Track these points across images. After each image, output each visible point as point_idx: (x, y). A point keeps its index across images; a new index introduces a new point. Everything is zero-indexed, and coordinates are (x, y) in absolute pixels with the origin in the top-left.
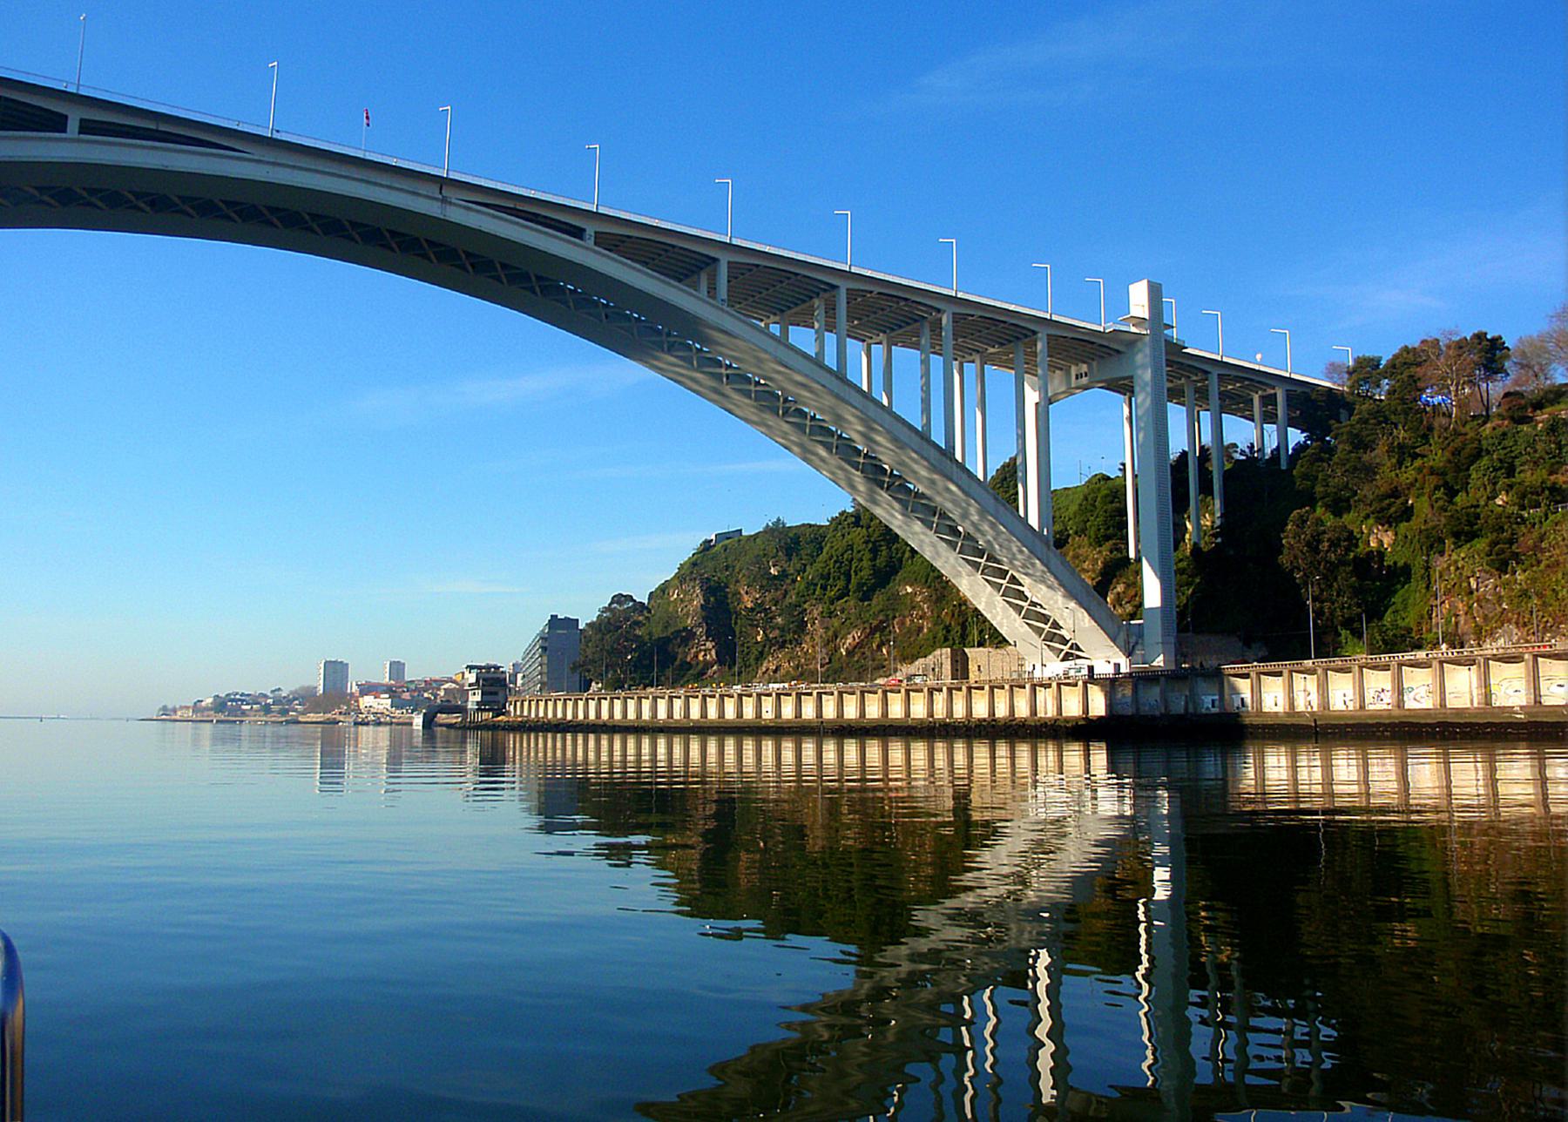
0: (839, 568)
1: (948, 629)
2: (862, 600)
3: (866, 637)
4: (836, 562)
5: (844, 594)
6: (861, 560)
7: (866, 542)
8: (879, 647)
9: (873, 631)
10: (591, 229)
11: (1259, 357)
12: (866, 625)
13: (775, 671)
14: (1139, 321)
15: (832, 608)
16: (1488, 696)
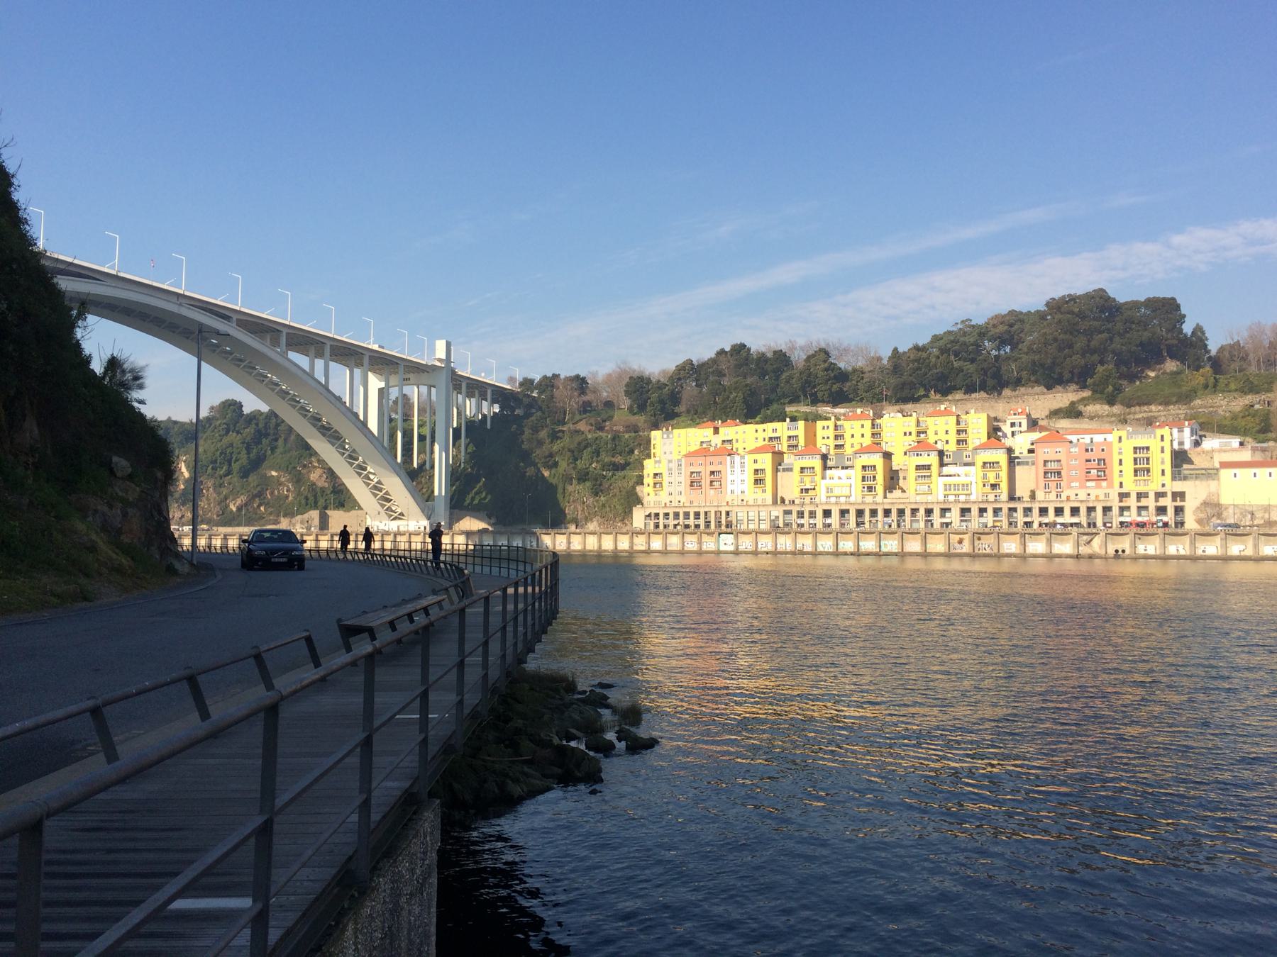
0: (224, 458)
1: (307, 498)
2: (242, 477)
3: (250, 500)
4: (221, 453)
5: (229, 473)
6: (239, 453)
7: (243, 443)
8: (259, 506)
9: (254, 496)
10: (235, 317)
11: (483, 374)
12: (250, 493)
13: (180, 518)
14: (440, 360)
15: (221, 481)
16: (600, 546)
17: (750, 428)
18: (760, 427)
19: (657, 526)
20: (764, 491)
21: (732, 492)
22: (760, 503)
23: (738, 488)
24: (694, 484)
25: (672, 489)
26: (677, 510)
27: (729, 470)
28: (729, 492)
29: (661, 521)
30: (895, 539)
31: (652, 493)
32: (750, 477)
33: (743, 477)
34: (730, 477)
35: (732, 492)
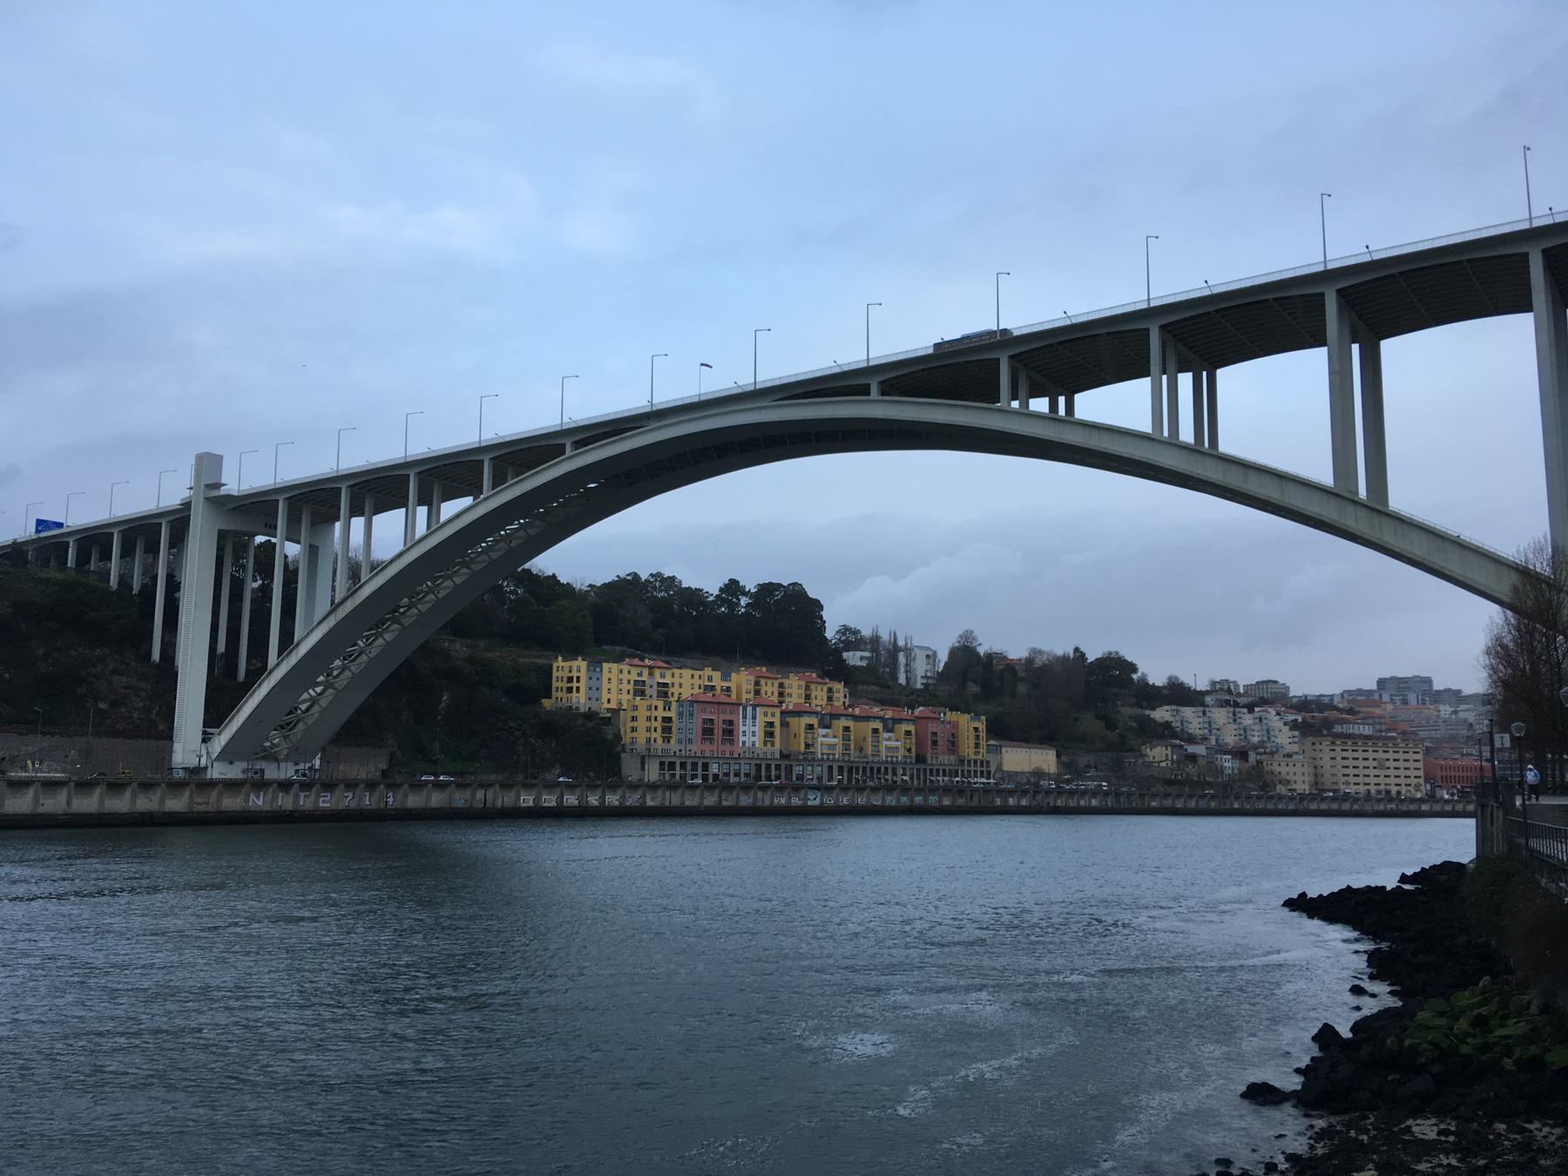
17: (687, 673)
18: (697, 673)
19: (673, 776)
20: (773, 744)
21: (744, 743)
22: (769, 757)
23: (749, 740)
24: (708, 732)
25: (683, 736)
26: (696, 760)
27: (741, 720)
28: (741, 745)
29: (678, 772)
30: (935, 795)
31: (660, 741)
32: (759, 728)
33: (753, 729)
34: (742, 728)
35: (744, 743)
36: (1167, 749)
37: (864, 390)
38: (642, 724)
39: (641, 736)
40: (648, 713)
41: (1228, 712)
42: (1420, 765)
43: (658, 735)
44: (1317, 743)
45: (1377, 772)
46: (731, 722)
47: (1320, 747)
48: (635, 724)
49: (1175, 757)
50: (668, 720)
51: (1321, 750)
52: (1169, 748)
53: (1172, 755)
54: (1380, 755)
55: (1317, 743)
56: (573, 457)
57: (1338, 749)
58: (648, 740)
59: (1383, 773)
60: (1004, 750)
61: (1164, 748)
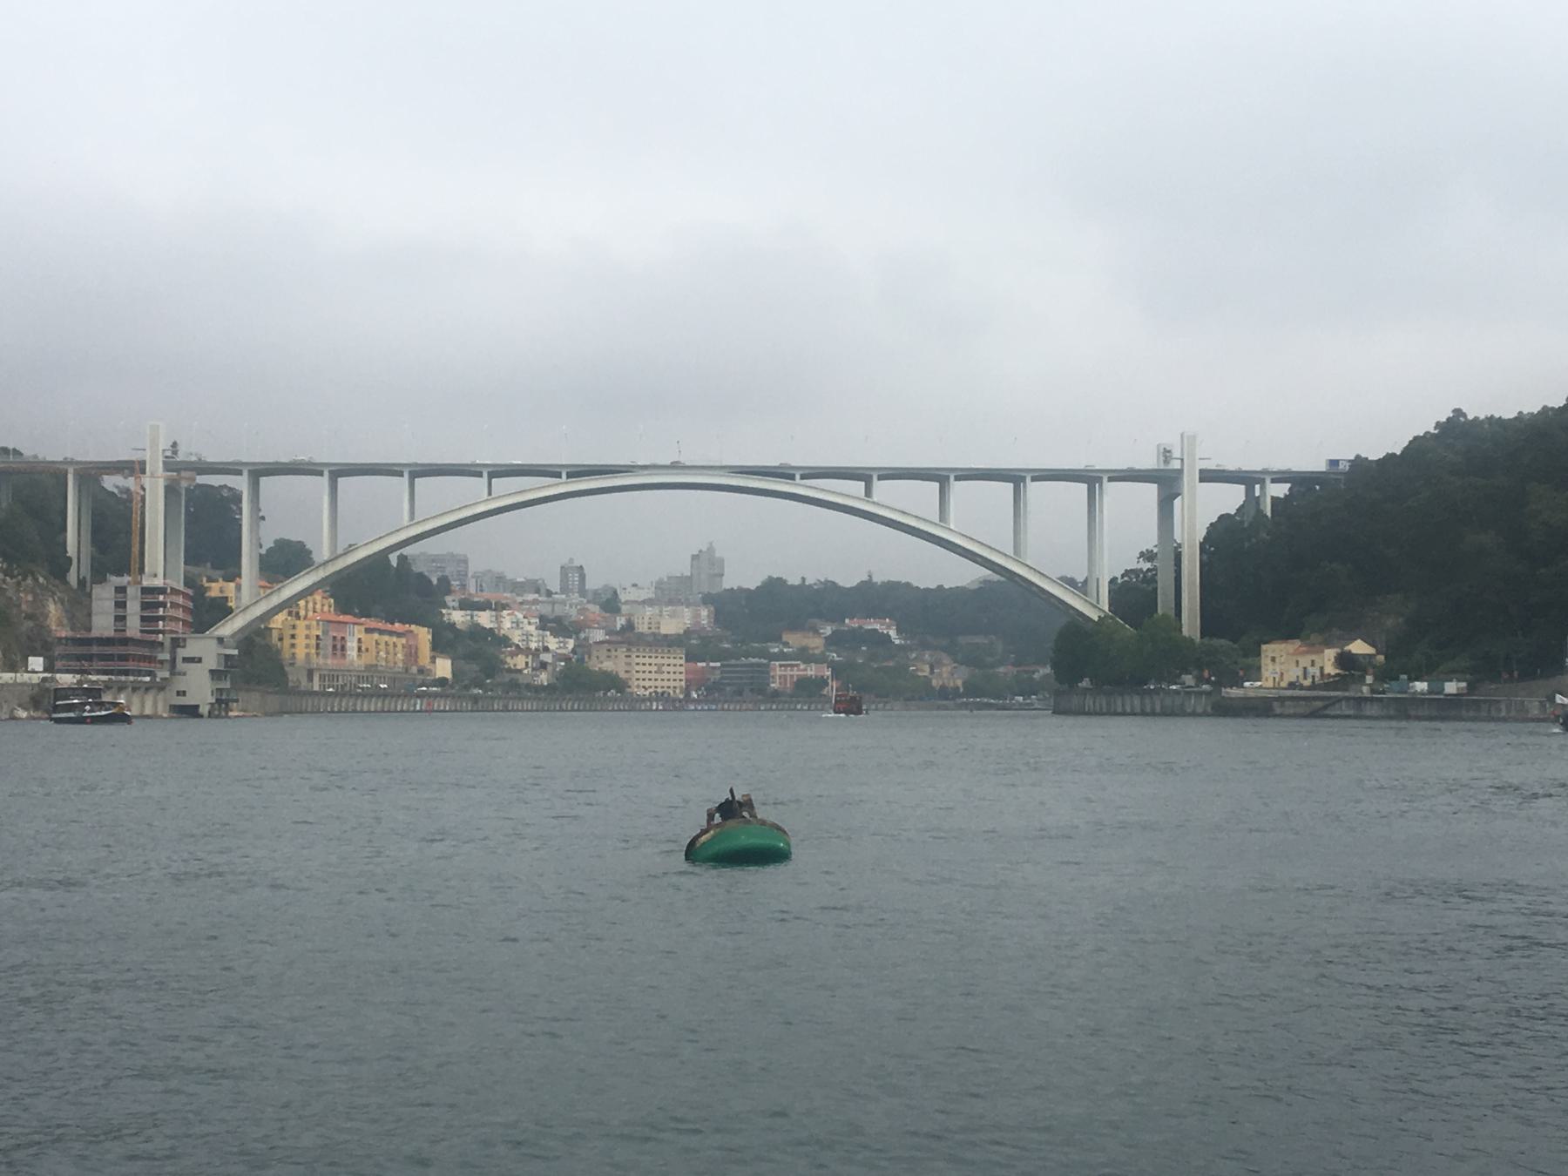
32: (355, 645)
36: (527, 657)
37: (792, 477)
38: (301, 641)
39: (301, 652)
40: (308, 632)
41: (492, 616)
42: (682, 669)
43: (313, 651)
44: (613, 650)
45: (657, 676)
46: (343, 638)
47: (616, 654)
48: (293, 641)
49: (534, 665)
50: (318, 636)
51: (616, 657)
52: (530, 657)
53: (533, 661)
54: (659, 661)
55: (613, 650)
56: (566, 483)
57: (634, 656)
58: (308, 655)
59: (659, 676)
60: (438, 660)
61: (524, 657)
